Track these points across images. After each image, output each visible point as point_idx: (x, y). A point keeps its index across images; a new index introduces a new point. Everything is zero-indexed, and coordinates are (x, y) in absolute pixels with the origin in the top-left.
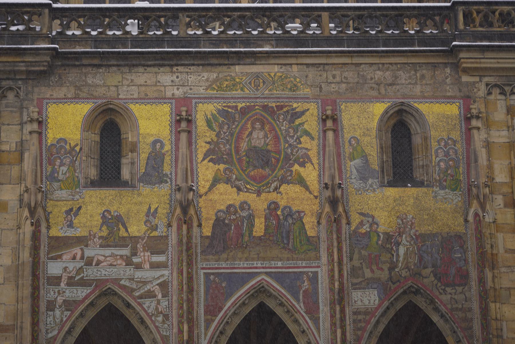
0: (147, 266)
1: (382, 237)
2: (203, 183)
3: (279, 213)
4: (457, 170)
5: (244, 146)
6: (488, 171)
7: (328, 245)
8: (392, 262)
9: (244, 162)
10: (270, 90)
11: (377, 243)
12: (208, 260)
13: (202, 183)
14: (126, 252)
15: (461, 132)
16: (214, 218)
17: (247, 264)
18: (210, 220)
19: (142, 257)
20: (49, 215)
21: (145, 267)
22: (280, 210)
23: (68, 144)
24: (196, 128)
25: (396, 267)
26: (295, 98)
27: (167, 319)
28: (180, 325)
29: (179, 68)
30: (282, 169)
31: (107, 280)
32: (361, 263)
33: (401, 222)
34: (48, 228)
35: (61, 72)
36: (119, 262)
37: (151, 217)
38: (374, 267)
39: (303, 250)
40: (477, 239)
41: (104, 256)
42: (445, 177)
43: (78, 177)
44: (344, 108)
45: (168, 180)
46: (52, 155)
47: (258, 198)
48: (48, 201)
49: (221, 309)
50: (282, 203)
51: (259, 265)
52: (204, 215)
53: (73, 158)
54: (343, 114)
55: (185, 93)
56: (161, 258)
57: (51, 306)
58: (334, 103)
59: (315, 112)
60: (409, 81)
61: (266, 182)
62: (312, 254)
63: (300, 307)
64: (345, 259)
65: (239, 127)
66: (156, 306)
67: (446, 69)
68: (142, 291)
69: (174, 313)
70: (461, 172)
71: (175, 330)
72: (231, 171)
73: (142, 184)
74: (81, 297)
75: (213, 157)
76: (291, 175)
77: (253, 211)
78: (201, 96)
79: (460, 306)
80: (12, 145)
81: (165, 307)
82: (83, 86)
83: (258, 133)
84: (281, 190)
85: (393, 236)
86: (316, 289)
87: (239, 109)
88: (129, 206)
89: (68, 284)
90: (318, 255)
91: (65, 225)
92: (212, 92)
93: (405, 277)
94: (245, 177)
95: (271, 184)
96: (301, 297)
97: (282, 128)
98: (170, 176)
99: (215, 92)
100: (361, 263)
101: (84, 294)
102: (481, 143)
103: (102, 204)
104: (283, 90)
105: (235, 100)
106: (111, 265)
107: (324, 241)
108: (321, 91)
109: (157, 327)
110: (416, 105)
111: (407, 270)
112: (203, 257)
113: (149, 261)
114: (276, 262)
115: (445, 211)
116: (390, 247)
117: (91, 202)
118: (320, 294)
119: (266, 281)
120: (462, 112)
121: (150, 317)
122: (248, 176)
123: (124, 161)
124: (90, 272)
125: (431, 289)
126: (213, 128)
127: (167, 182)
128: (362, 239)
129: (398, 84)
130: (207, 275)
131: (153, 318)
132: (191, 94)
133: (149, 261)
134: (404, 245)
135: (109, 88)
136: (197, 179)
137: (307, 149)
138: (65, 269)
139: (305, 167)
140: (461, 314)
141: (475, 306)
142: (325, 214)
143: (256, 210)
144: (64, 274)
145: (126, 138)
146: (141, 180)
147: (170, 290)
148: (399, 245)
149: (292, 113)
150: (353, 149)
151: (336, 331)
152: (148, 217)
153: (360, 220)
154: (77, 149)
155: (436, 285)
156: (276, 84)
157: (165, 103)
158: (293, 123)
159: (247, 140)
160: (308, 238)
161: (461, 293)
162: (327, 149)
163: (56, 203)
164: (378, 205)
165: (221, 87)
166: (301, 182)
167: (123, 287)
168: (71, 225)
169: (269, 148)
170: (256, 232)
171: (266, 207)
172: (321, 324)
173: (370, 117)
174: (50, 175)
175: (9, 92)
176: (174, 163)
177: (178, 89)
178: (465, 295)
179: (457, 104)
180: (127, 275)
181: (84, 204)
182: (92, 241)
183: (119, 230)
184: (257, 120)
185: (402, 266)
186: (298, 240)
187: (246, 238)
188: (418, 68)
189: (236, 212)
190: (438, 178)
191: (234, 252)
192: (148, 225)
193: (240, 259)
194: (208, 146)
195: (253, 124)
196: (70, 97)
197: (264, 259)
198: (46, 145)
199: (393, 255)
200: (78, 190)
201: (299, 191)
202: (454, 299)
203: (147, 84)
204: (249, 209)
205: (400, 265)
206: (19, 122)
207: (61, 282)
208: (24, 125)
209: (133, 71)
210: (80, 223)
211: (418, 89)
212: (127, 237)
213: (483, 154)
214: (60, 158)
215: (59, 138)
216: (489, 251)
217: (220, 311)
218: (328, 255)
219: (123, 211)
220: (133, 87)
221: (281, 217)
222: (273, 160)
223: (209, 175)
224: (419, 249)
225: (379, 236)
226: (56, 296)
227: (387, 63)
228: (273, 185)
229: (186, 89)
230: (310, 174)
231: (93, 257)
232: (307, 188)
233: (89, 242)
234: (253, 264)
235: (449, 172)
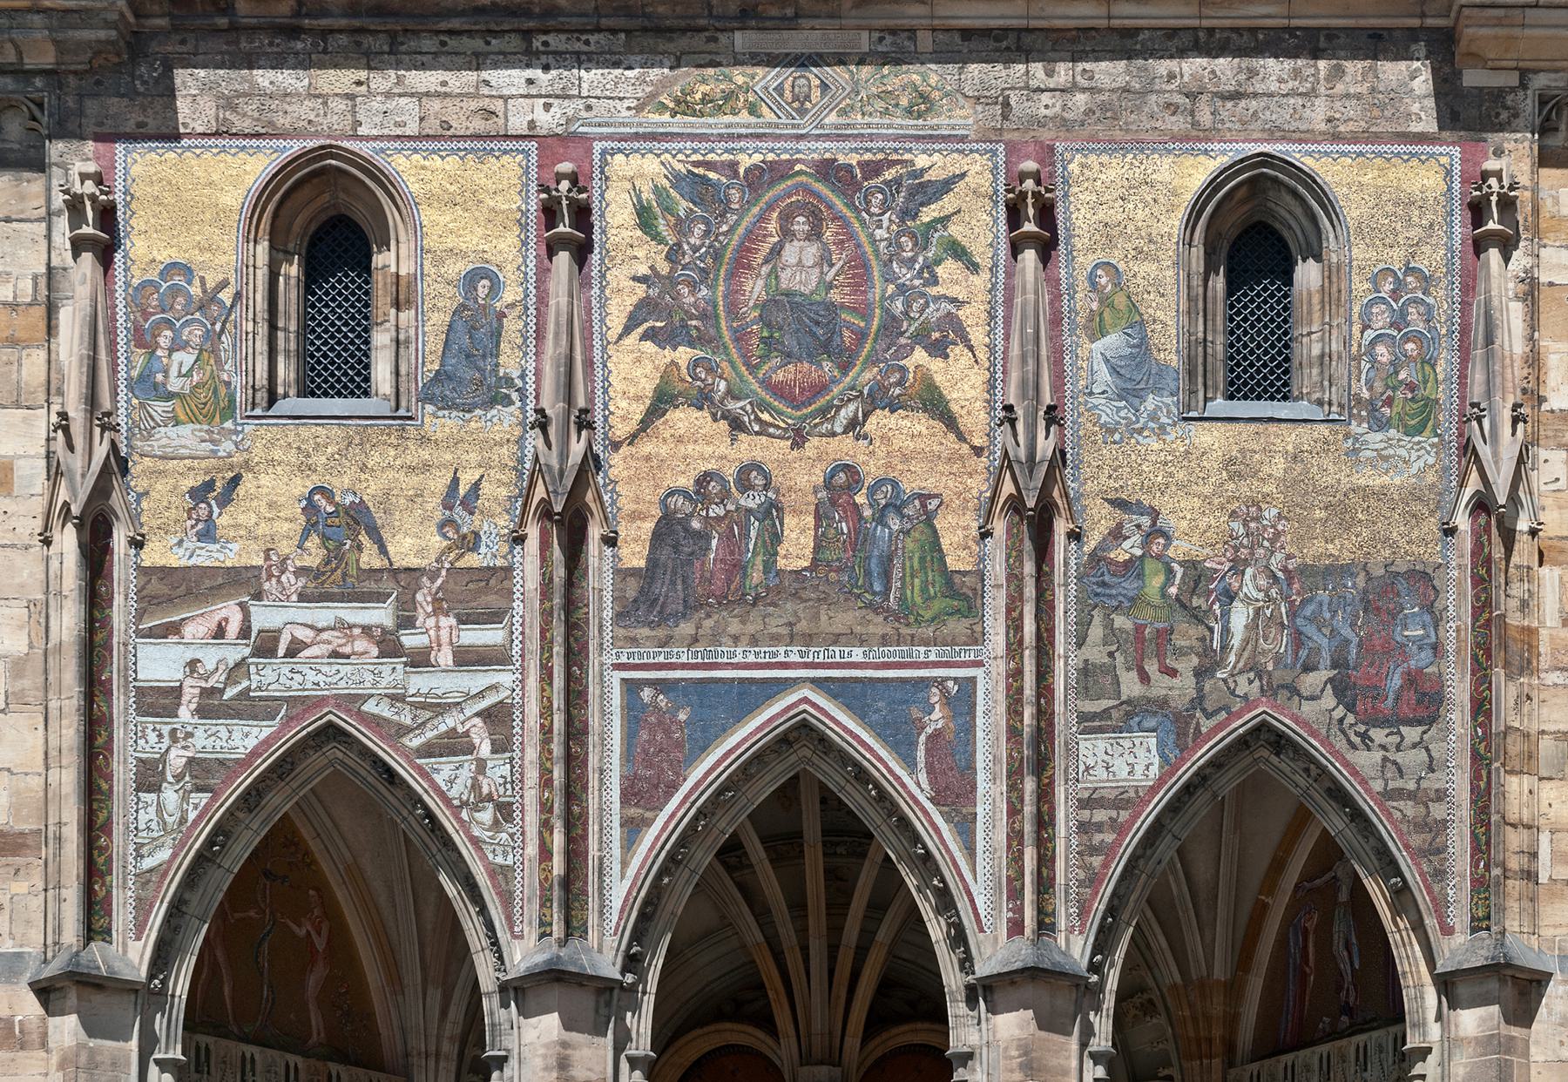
0: (445, 657)
1: (1179, 576)
2: (624, 404)
3: (860, 499)
4: (1427, 368)
5: (755, 288)
6: (1525, 372)
7: (1009, 596)
8: (1206, 651)
9: (755, 341)
10: (843, 113)
11: (1164, 595)
12: (634, 641)
13: (620, 405)
14: (380, 615)
15: (1450, 249)
16: (657, 512)
17: (757, 654)
18: (643, 519)
19: (432, 632)
20: (138, 502)
21: (441, 661)
22: (864, 491)
23: (197, 282)
24: (604, 232)
25: (1219, 664)
26: (924, 137)
27: (509, 818)
28: (546, 835)
29: (550, 38)
30: (874, 364)
31: (322, 701)
32: (1111, 654)
33: (1242, 531)
34: (138, 544)
35: (170, 49)
36: (361, 645)
37: (458, 509)
38: (1152, 667)
39: (928, 615)
40: (1478, 581)
41: (311, 627)
42: (1389, 392)
43: (228, 384)
44: (1077, 172)
45: (515, 396)
46: (146, 315)
47: (795, 453)
48: (136, 457)
49: (673, 787)
50: (872, 469)
51: (794, 658)
52: (626, 504)
53: (213, 324)
54: (1075, 190)
55: (568, 121)
56: (489, 636)
57: (149, 777)
58: (1047, 153)
59: (985, 182)
60: (1291, 84)
61: (821, 402)
62: (957, 626)
63: (918, 785)
64: (1060, 638)
65: (740, 231)
66: (475, 779)
67: (1413, 47)
68: (430, 735)
69: (527, 801)
70: (1441, 377)
71: (532, 850)
72: (710, 370)
73: (429, 408)
74: (242, 750)
75: (659, 324)
76: (899, 383)
77: (777, 492)
78: (622, 130)
79: (1412, 786)
80: (21, 285)
81: (501, 781)
82: (245, 95)
83: (802, 249)
84: (867, 427)
85: (1216, 571)
86: (970, 728)
87: (742, 171)
88: (391, 474)
89: (202, 712)
90: (978, 628)
91: (192, 533)
92: (655, 118)
93: (1245, 697)
94: (755, 386)
95: (839, 408)
96: (921, 754)
97: (880, 233)
98: (519, 383)
99: (666, 117)
100: (1111, 654)
101: (251, 743)
102: (1511, 285)
103: (306, 468)
104: (886, 112)
105: (731, 145)
106: (335, 654)
107: (999, 586)
108: (1005, 117)
109: (476, 842)
110: (1308, 163)
111: (1252, 675)
112: (621, 632)
113: (451, 643)
114: (847, 650)
115: (1381, 494)
116: (1204, 607)
117: (272, 462)
118: (979, 744)
119: (814, 705)
120: (1457, 186)
121: (455, 812)
122: (766, 384)
123: (381, 339)
124: (269, 675)
125: (1324, 731)
126: (659, 234)
127: (508, 401)
128: (1115, 580)
129: (1255, 95)
130: (631, 687)
131: (464, 815)
132: (590, 125)
133: (451, 643)
134: (1248, 600)
135: (325, 103)
136: (605, 392)
137: (954, 300)
138: (193, 664)
139: (946, 357)
140: (1409, 808)
141: (1460, 784)
142: (1002, 501)
143: (790, 489)
144: (189, 682)
145: (385, 267)
146: (426, 398)
147: (517, 729)
148: (1232, 599)
149: (910, 187)
150: (1101, 302)
151: (1021, 852)
152: (451, 509)
153: (1112, 524)
154: (226, 296)
155: (1341, 721)
156: (863, 94)
157: (505, 152)
158: (915, 217)
159: (765, 270)
160: (948, 576)
161: (1414, 746)
162: (1018, 300)
163: (161, 465)
164: (1171, 475)
165: (686, 102)
166: (935, 405)
167: (376, 722)
168: (208, 534)
169: (835, 296)
170: (785, 557)
171: (819, 479)
172: (980, 835)
173: (1162, 199)
174: (140, 375)
175: (10, 113)
176: (532, 342)
177: (547, 107)
178: (1427, 750)
179: (1444, 160)
180: (384, 684)
181: (249, 469)
182: (274, 580)
183: (360, 548)
184: (800, 208)
185: (1237, 662)
186: (917, 581)
187: (756, 576)
188: (1322, 44)
189: (725, 496)
190: (1366, 394)
191: (716, 617)
192: (450, 534)
193: (736, 639)
194: (641, 290)
195: (786, 218)
196: (200, 129)
197: (809, 639)
198: (127, 284)
199: (1211, 630)
200: (229, 424)
201: (925, 431)
202: (1395, 763)
203: (447, 89)
204: (766, 487)
205: (1232, 658)
206: (43, 212)
207: (179, 705)
208: (55, 219)
209: (403, 48)
210: (237, 526)
211: (1317, 114)
212: (380, 571)
213: (1515, 316)
214: (169, 324)
215: (168, 261)
216: (1514, 620)
217: (669, 795)
218: (1008, 627)
219: (371, 490)
220: (403, 101)
221: (867, 513)
222: (846, 333)
223: (644, 380)
224: (1293, 613)
225: (1170, 572)
226: (164, 747)
227: (1223, 29)
228: (843, 412)
229: (572, 107)
230: (962, 380)
231: (279, 631)
232: (950, 422)
233: (266, 586)
234: (775, 655)
235: (1402, 375)
